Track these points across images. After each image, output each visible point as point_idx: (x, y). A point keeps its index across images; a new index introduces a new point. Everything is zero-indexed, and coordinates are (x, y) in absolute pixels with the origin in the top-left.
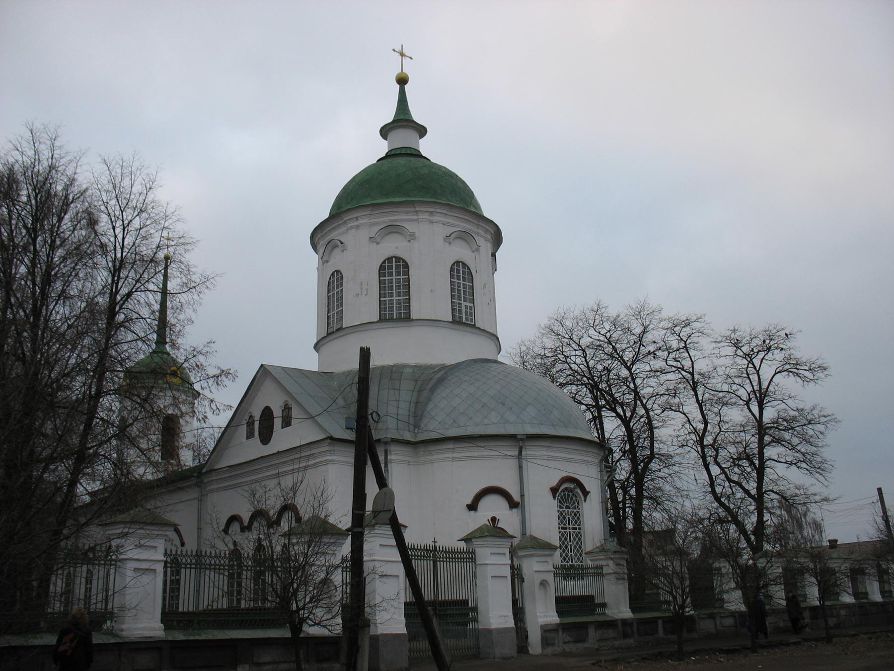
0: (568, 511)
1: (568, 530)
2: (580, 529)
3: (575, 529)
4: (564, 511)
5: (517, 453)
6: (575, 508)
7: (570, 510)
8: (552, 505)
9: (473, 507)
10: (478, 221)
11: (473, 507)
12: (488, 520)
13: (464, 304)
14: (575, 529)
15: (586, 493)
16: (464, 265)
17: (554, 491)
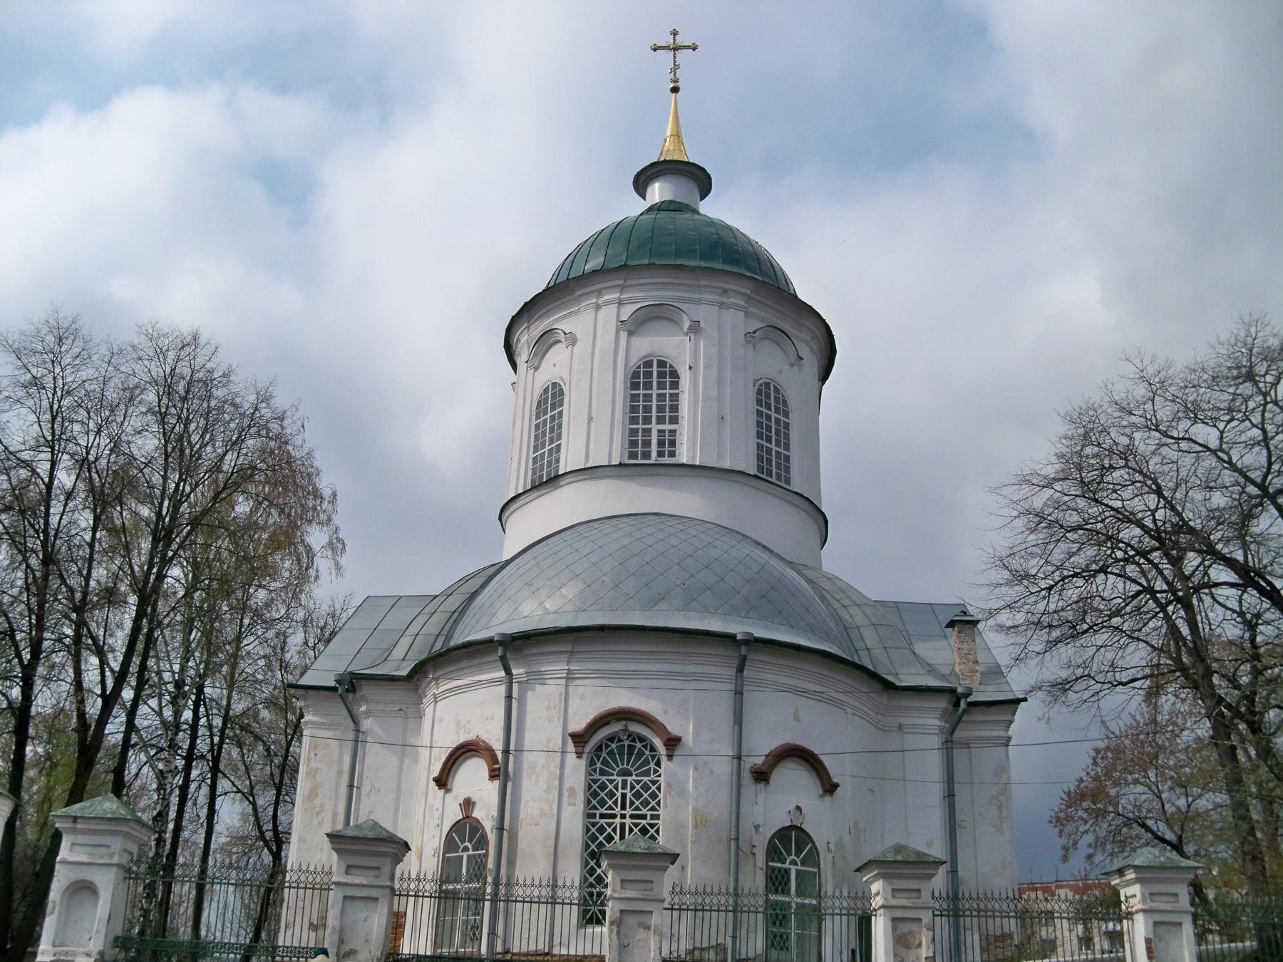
0: (624, 783)
1: (618, 821)
2: (590, 816)
3: (644, 817)
4: (611, 782)
5: (502, 674)
6: (647, 773)
7: (629, 779)
8: (576, 769)
9: (442, 781)
10: (698, 280)
11: (442, 781)
12: (460, 805)
13: (655, 427)
14: (644, 817)
15: (673, 743)
16: (662, 364)
17: (579, 739)
